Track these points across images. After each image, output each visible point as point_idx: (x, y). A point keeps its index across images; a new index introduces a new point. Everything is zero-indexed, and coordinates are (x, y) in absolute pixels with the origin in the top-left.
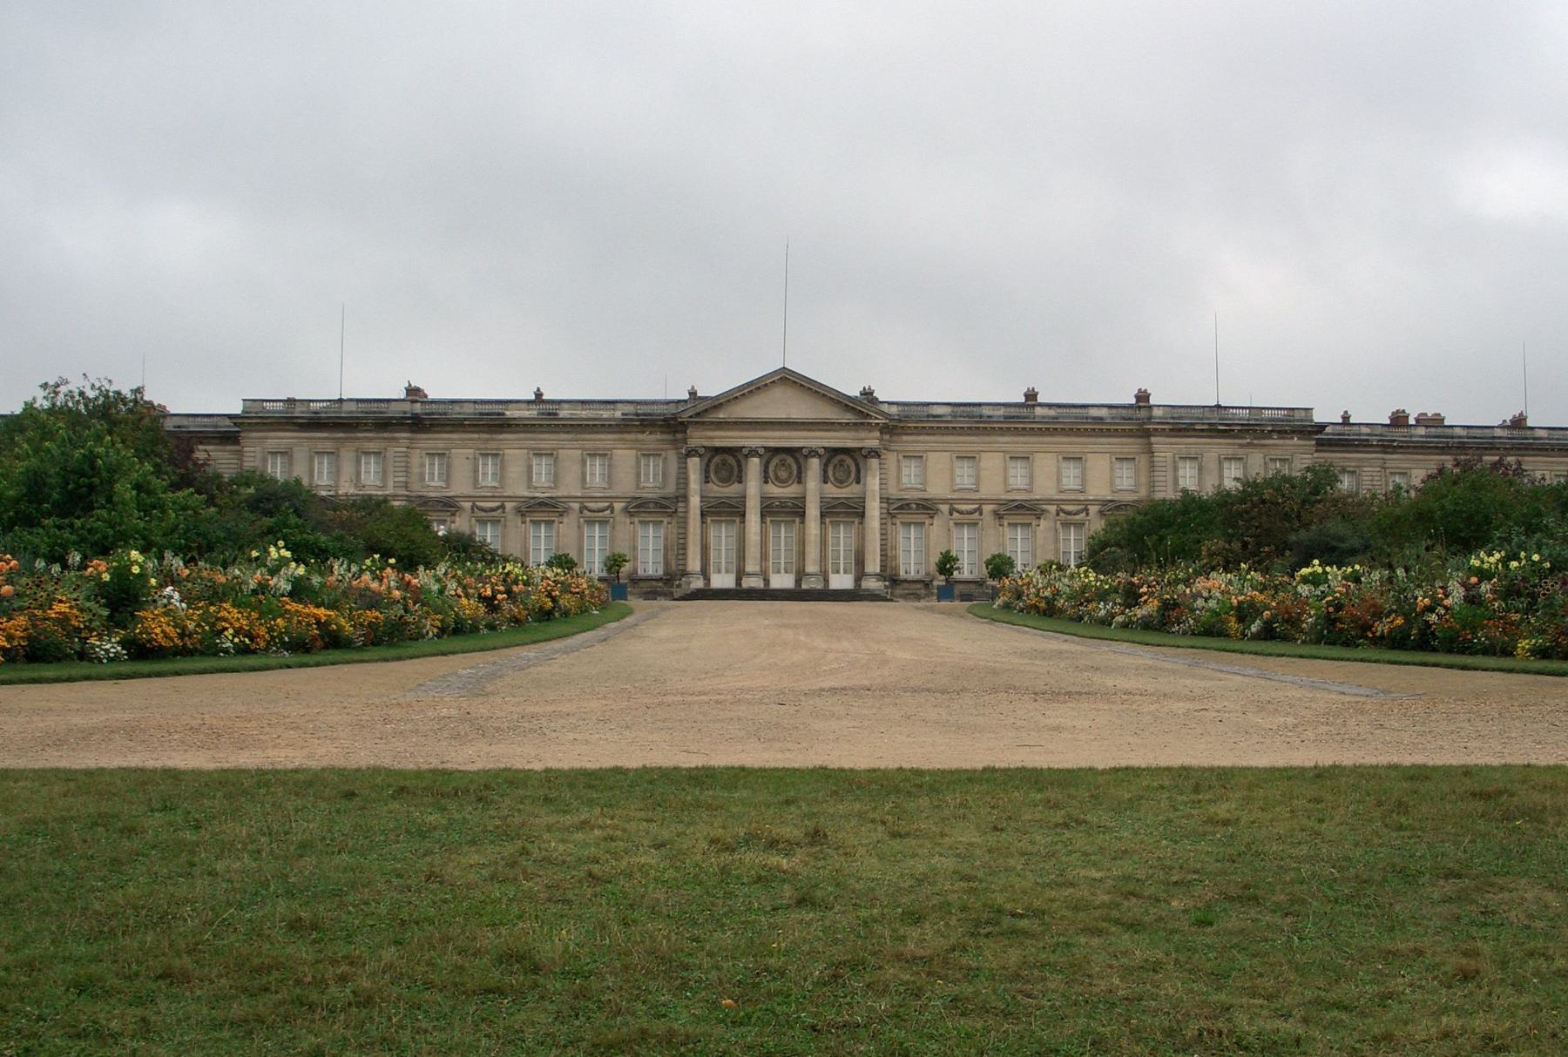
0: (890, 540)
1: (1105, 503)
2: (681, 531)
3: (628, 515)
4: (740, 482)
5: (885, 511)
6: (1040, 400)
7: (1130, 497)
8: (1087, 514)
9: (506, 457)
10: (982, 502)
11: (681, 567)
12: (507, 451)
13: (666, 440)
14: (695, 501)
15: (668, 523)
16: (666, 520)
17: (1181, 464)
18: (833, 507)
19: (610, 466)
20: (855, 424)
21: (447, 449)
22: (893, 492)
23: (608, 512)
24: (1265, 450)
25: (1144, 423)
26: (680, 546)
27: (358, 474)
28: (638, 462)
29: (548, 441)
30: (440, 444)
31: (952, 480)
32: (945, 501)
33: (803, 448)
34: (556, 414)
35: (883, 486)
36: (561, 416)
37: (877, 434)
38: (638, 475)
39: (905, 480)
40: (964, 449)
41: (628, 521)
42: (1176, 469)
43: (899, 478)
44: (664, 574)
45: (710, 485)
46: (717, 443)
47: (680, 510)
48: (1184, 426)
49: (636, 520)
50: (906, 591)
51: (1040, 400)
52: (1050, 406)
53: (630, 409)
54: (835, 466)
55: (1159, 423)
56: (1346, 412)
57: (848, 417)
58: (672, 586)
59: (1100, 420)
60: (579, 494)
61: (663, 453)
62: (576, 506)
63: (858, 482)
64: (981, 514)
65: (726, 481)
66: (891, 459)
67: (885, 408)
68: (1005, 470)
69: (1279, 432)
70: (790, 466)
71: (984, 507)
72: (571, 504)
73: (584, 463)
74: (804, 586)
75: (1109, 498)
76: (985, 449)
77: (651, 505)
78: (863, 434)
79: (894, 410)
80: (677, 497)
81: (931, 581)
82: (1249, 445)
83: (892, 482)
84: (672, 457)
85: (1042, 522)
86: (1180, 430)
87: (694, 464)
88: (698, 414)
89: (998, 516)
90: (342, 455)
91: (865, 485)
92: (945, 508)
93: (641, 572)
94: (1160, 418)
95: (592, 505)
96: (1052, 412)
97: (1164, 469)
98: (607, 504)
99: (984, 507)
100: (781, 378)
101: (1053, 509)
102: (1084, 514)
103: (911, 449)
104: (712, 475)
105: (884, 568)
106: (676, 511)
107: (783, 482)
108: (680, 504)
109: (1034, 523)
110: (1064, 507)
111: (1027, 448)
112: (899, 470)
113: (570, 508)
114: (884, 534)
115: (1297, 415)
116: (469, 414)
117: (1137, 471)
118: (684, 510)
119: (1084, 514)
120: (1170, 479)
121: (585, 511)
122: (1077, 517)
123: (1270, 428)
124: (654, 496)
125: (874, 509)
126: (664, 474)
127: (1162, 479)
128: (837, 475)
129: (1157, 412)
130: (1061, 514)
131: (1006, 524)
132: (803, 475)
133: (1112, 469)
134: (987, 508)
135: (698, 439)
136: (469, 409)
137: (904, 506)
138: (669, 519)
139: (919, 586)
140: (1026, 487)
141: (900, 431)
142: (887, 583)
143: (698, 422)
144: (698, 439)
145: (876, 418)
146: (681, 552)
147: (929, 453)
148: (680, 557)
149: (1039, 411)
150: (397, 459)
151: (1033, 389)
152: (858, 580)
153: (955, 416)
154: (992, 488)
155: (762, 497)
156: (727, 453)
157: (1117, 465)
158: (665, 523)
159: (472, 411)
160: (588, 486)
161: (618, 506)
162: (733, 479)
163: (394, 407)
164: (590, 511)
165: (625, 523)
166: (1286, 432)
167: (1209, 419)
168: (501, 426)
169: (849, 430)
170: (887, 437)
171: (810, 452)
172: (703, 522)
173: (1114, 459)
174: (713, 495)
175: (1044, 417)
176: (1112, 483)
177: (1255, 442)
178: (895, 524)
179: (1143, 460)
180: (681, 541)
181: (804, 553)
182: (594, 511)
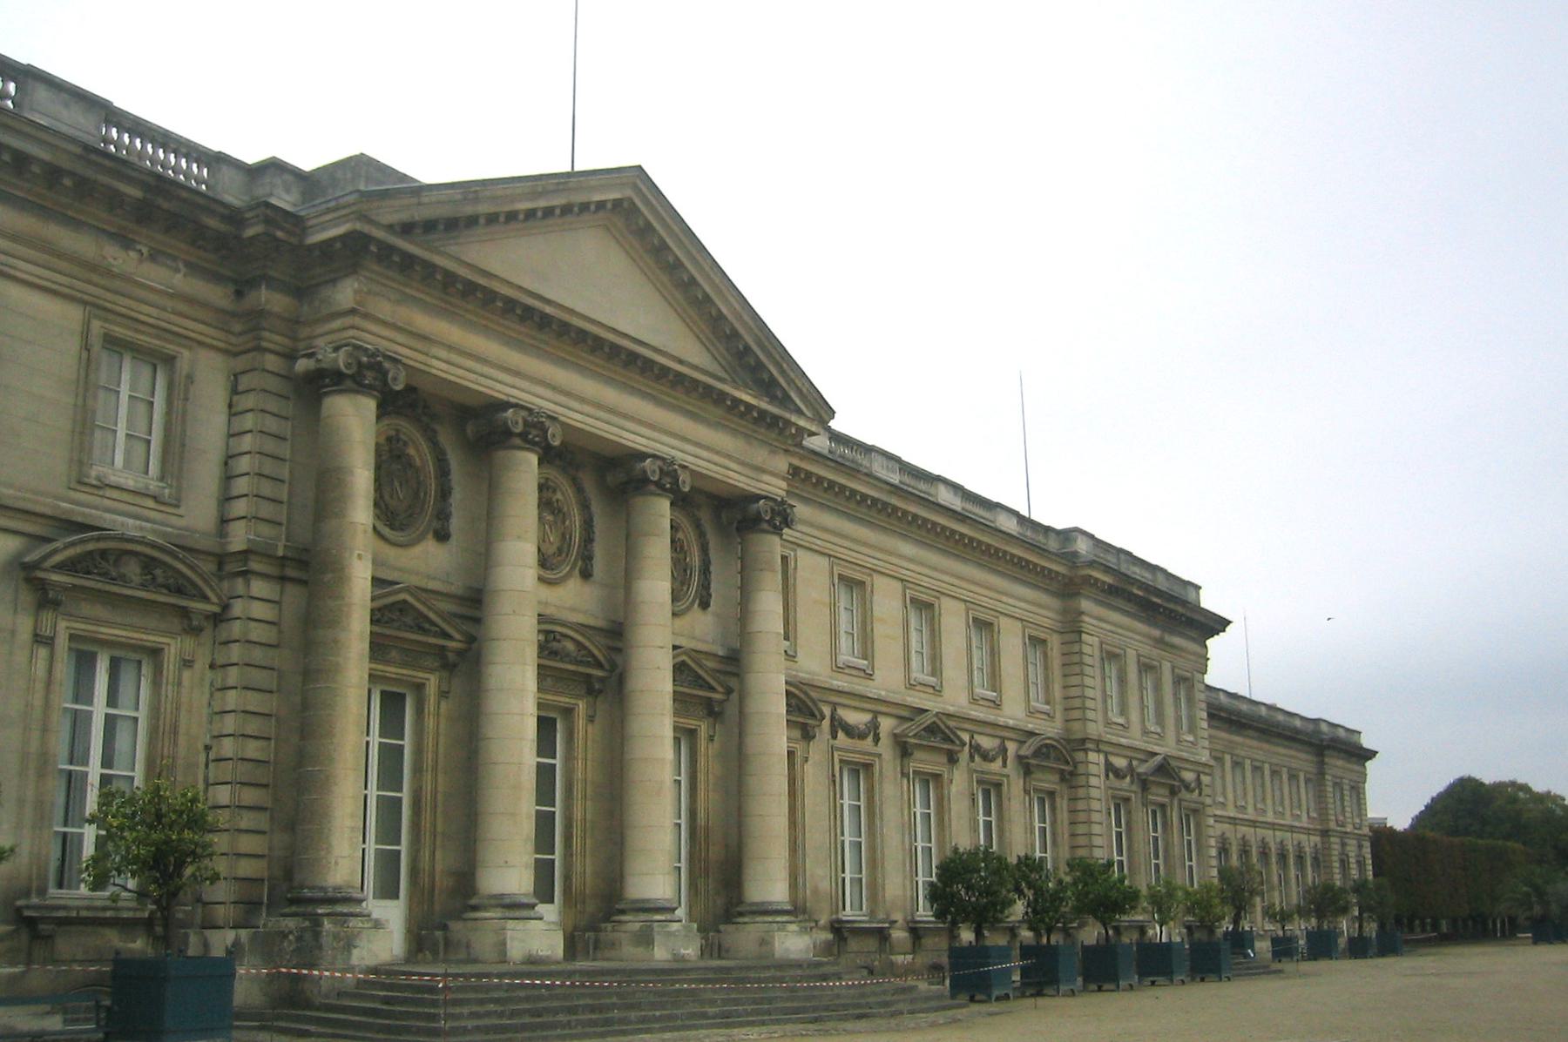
3: (27, 597)
8: (1004, 764)
10: (875, 706)
13: (204, 305)
15: (187, 663)
47: (238, 608)
61: (186, 353)
63: (705, 605)
70: (560, 510)
78: (760, 455)
89: (904, 749)
100: (617, 203)
102: (999, 761)
106: (219, 618)
138: (189, 643)
145: (799, 412)
147: (800, 552)
165: (13, 632)
169: (734, 432)
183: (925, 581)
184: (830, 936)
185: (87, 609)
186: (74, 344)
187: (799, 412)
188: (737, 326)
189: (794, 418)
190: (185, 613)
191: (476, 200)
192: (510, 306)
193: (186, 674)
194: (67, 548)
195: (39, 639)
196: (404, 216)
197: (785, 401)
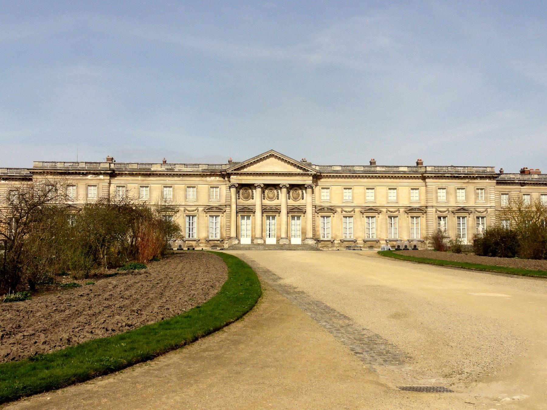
0: (316, 223)
1: (406, 207)
2: (229, 219)
4: (253, 199)
5: (314, 211)
6: (377, 164)
7: (416, 205)
8: (399, 212)
9: (152, 188)
10: (355, 207)
11: (228, 235)
12: (152, 185)
14: (234, 207)
16: (221, 215)
17: (439, 191)
18: (292, 209)
19: (197, 192)
20: (302, 174)
21: (126, 184)
22: (317, 203)
23: (196, 211)
24: (474, 185)
25: (424, 174)
26: (227, 226)
27: (87, 195)
28: (209, 190)
29: (169, 180)
30: (123, 182)
31: (343, 197)
32: (339, 207)
33: (280, 184)
34: (173, 169)
35: (313, 201)
36: (175, 170)
37: (311, 178)
38: (209, 196)
39: (322, 198)
40: (347, 185)
41: (205, 215)
42: (437, 193)
43: (320, 198)
44: (220, 239)
45: (240, 200)
46: (243, 182)
48: (440, 175)
49: (208, 215)
50: (323, 245)
51: (377, 164)
52: (383, 166)
53: (205, 167)
54: (293, 192)
55: (429, 174)
56: (501, 169)
57: (299, 171)
58: (224, 243)
59: (404, 172)
60: (184, 204)
62: (182, 209)
63: (303, 199)
64: (354, 212)
65: (247, 198)
66: (317, 189)
67: (314, 167)
68: (365, 193)
69: (480, 177)
71: (355, 209)
72: (180, 208)
73: (186, 191)
74: (281, 243)
75: (408, 205)
76: (356, 185)
77: (215, 209)
78: (305, 178)
79: (317, 168)
80: (226, 206)
81: (334, 241)
82: (468, 182)
83: (317, 199)
84: (224, 189)
85: (380, 215)
86: (438, 176)
87: (233, 190)
88: (235, 170)
90: (79, 186)
91: (306, 200)
92: (339, 210)
93: (210, 238)
94: (430, 171)
95: (189, 209)
96: (384, 169)
97: (432, 193)
98: (196, 208)
99: (355, 209)
101: (384, 210)
102: (398, 212)
103: (325, 184)
104: (241, 195)
105: (314, 235)
107: (271, 199)
108: (227, 208)
109: (377, 216)
110: (389, 209)
111: (374, 184)
112: (320, 193)
113: (180, 210)
114: (314, 221)
115: (488, 170)
116: (135, 169)
117: (420, 194)
118: (229, 211)
119: (398, 212)
120: (434, 197)
121: (186, 211)
122: (394, 213)
123: (477, 176)
124: (216, 204)
125: (309, 210)
126: (220, 195)
127: (431, 197)
128: (294, 195)
129: (429, 169)
130: (388, 212)
131: (365, 216)
132: (279, 196)
133: (410, 193)
134: (357, 210)
135: (235, 179)
136: (135, 166)
137: (322, 209)
139: (328, 243)
140: (372, 201)
141: (320, 177)
142: (315, 242)
143: (235, 173)
144: (235, 179)
146: (228, 228)
148: (227, 231)
149: (378, 169)
150: (104, 188)
151: (374, 160)
152: (303, 240)
153: (343, 171)
154: (359, 201)
155: (262, 205)
156: (247, 187)
157: (412, 191)
158: (220, 216)
159: (136, 168)
160: (187, 200)
161: (201, 209)
162: (250, 198)
163: (102, 166)
164: (188, 211)
166: (483, 177)
167: (450, 172)
168: (150, 174)
170: (315, 180)
171: (283, 186)
172: (237, 216)
173: (410, 189)
174: (241, 204)
175: (380, 171)
176: (409, 199)
177: (470, 181)
178: (317, 217)
179: (423, 189)
180: (228, 224)
181: (280, 229)
182: (190, 211)
183: (371, 185)
184: (340, 242)
185: (211, 213)
186: (207, 189)
187: (311, 172)
188: (296, 164)
189: (309, 173)
190: (221, 212)
191: (244, 164)
192: (251, 174)
193: (222, 217)
194: (208, 207)
195: (206, 216)
196: (234, 169)
197: (308, 171)
